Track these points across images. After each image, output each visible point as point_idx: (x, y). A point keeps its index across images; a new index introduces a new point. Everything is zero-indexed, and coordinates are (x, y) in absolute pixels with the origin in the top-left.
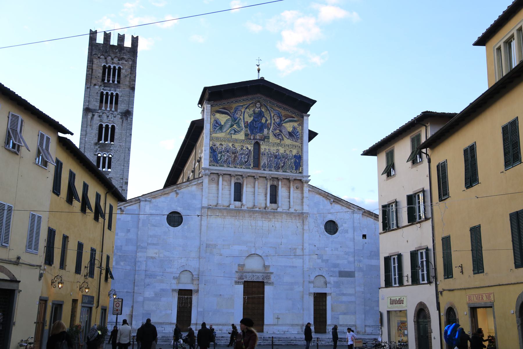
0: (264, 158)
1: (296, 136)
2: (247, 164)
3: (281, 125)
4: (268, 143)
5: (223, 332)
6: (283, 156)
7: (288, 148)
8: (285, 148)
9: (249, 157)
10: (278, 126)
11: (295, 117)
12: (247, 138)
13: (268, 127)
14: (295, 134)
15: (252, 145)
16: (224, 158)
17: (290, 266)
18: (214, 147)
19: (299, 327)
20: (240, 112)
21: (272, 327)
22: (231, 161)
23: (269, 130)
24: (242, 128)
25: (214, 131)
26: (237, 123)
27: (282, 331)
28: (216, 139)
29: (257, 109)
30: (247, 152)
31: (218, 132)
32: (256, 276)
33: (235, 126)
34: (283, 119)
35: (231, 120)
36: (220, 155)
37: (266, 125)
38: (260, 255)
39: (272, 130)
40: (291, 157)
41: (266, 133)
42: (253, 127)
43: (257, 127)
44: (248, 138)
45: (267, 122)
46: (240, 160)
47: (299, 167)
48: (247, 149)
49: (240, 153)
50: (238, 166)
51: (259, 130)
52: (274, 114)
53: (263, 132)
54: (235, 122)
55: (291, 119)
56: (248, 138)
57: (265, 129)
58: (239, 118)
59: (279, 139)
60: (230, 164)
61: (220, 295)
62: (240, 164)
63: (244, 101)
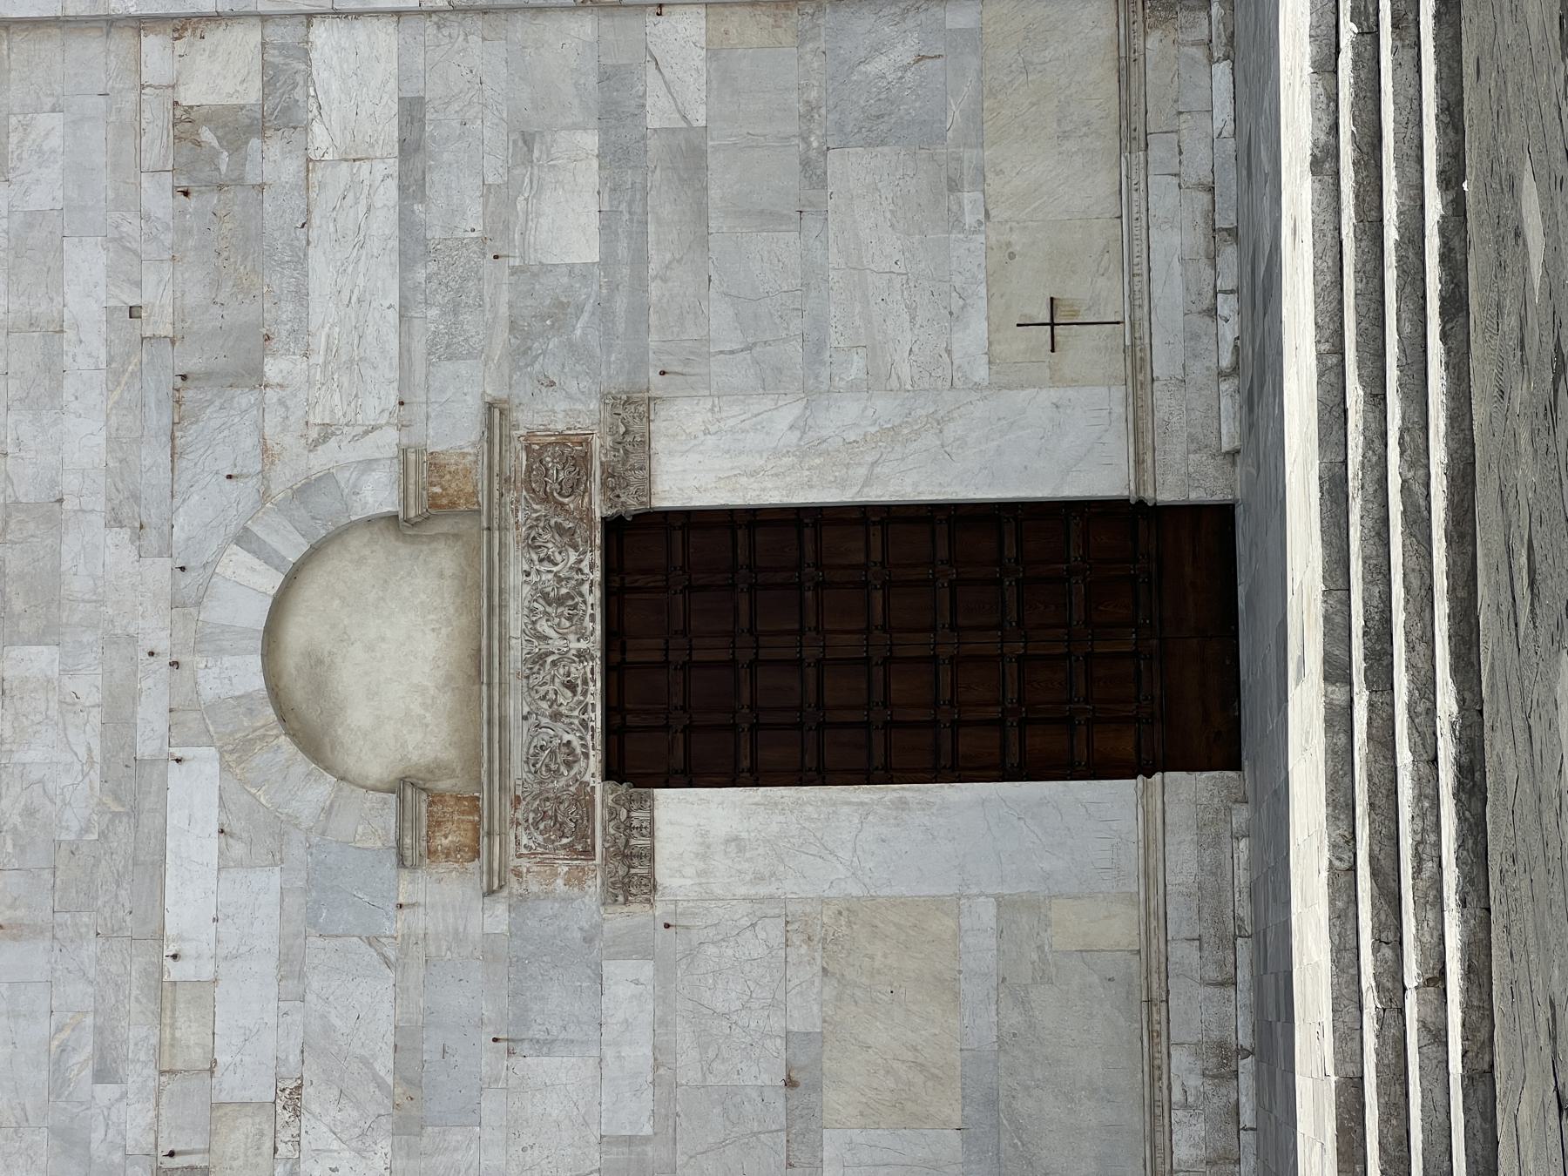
5: (1245, 1040)
17: (402, 188)
19: (1153, 42)
21: (1165, 402)
27: (1213, 259)
32: (544, 627)
38: (272, 581)
61: (790, 1083)
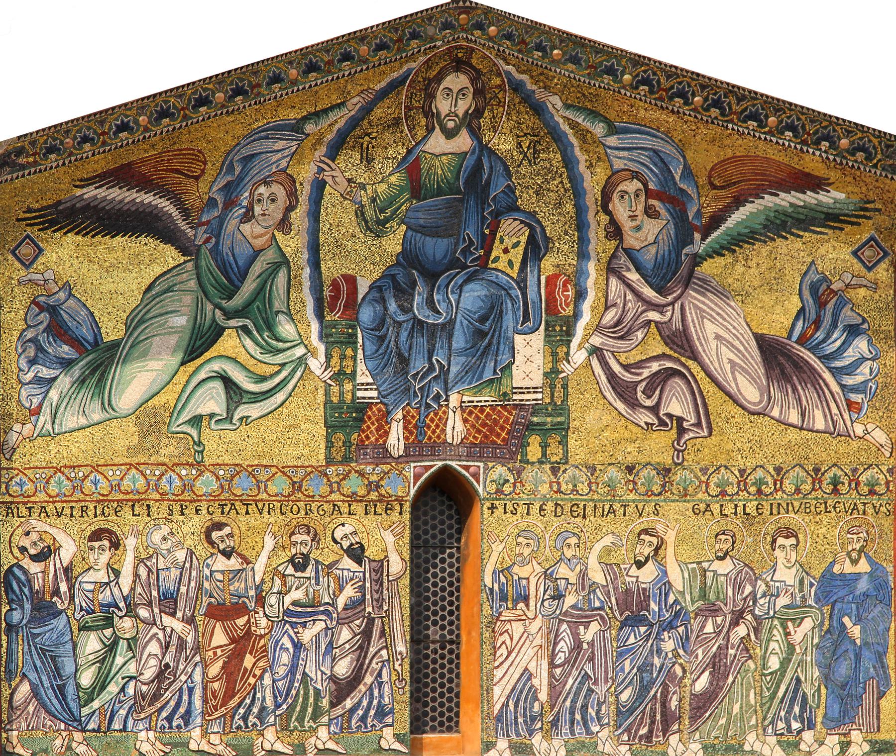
0: (517, 629)
1: (836, 372)
2: (349, 703)
3: (683, 270)
4: (554, 471)
6: (703, 595)
7: (751, 508)
8: (729, 509)
9: (367, 634)
10: (649, 292)
11: (833, 175)
12: (347, 444)
13: (552, 307)
14: (826, 359)
15: (395, 516)
16: (132, 669)
18: (35, 568)
20: (279, 190)
22: (198, 693)
23: (569, 334)
24: (300, 351)
25: (37, 412)
26: (249, 304)
28: (59, 483)
29: (437, 143)
30: (349, 592)
31: (71, 419)
33: (229, 343)
34: (708, 211)
35: (193, 284)
36: (92, 644)
37: (531, 294)
39: (596, 340)
40: (783, 601)
41: (537, 380)
42: (404, 335)
43: (448, 327)
44: (361, 445)
45: (548, 265)
46: (281, 671)
47: (868, 699)
48: (348, 563)
49: (288, 600)
50: (270, 734)
51: (462, 352)
52: (613, 174)
53: (509, 366)
54: (230, 298)
55: (786, 199)
56: (361, 445)
57: (519, 340)
58: (270, 255)
59: (662, 423)
60: (187, 717)
62: (291, 708)
63: (313, 75)
